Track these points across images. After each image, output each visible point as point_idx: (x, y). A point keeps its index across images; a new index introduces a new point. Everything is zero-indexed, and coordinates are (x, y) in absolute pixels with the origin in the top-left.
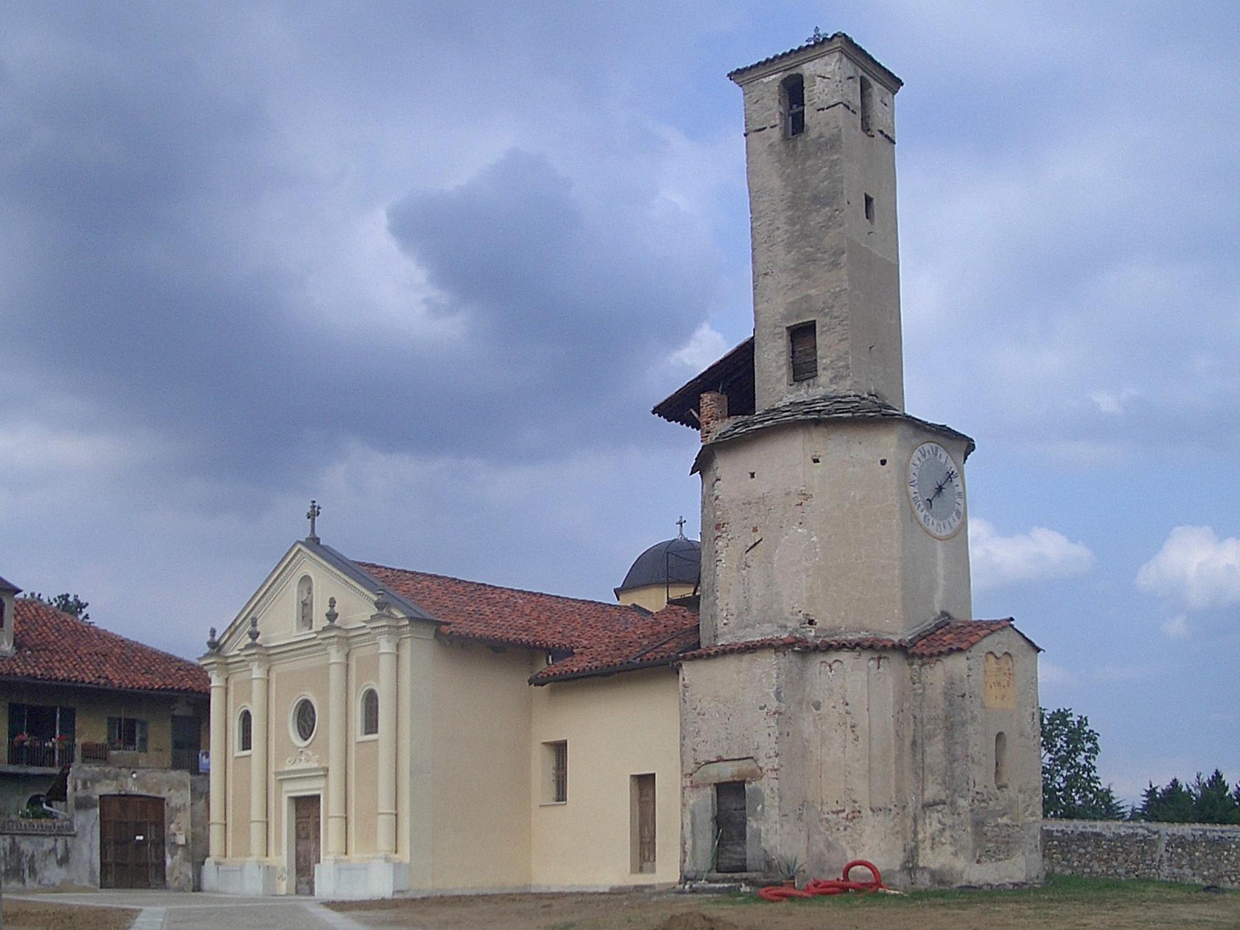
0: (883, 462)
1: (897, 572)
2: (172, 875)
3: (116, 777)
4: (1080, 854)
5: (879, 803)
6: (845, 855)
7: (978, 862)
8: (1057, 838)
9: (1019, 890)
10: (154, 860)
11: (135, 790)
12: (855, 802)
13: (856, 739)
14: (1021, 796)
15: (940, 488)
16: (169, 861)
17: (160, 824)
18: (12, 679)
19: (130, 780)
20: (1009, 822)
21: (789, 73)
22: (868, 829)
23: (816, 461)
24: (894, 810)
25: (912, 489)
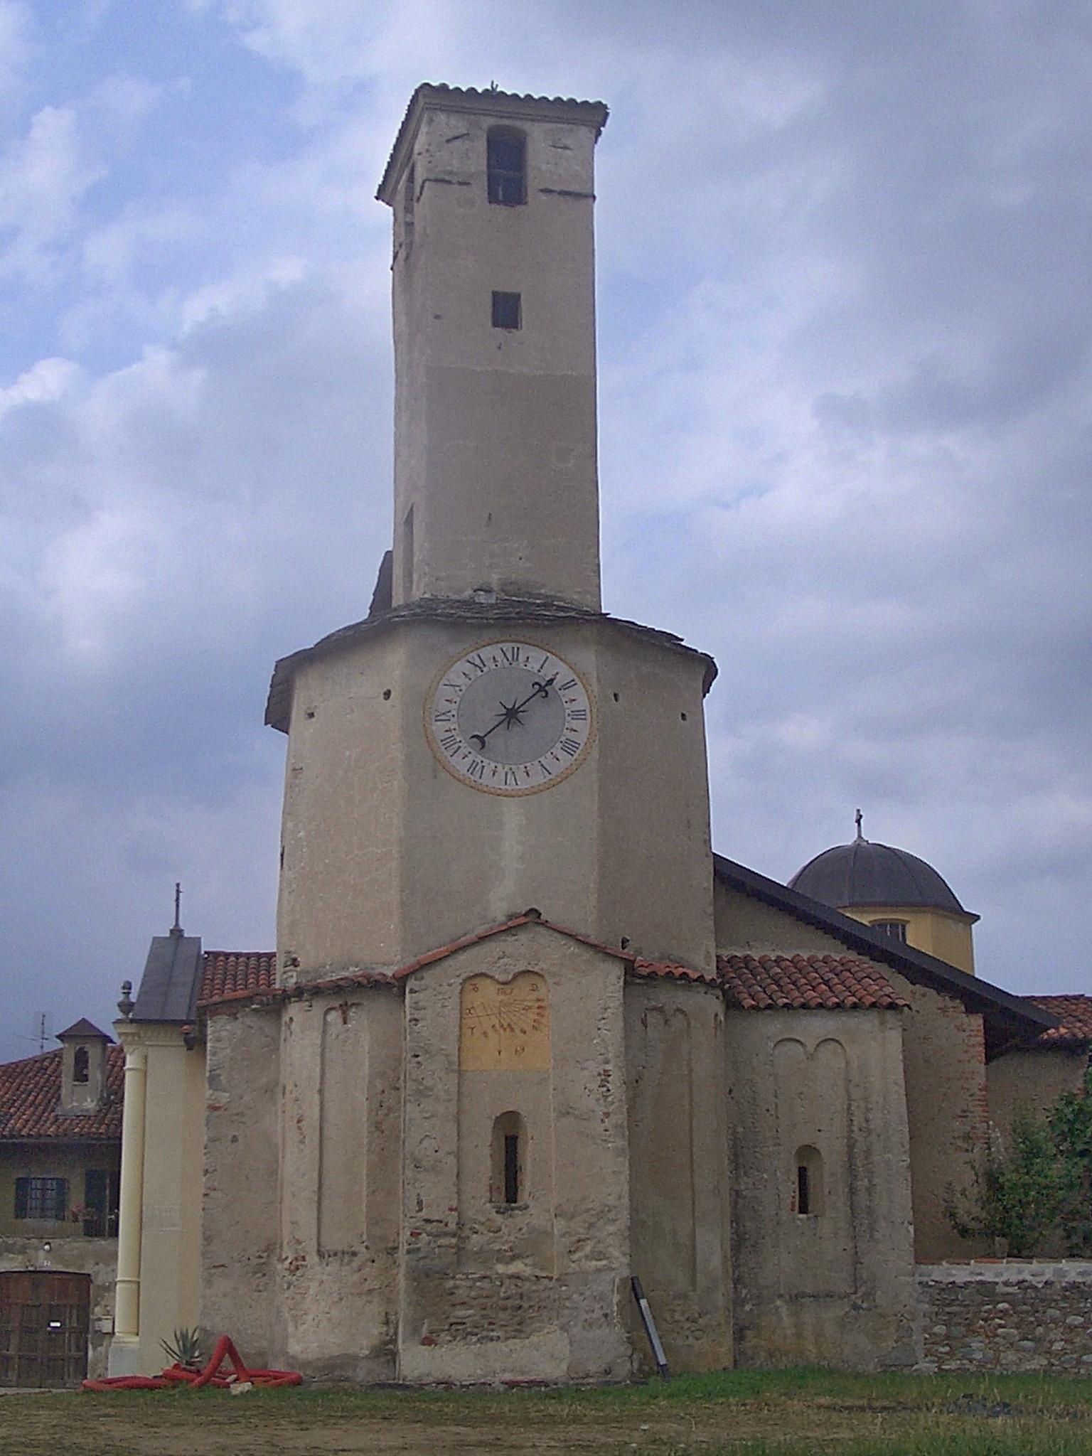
0: (387, 695)
1: (394, 864)
2: (94, 1370)
3: (23, 1250)
4: (1072, 1328)
5: (335, 1240)
6: (285, 1329)
7: (428, 1341)
8: (1006, 1297)
9: (572, 1389)
10: (73, 1353)
11: (47, 1264)
12: (299, 1242)
13: (302, 1142)
14: (560, 1225)
15: (512, 715)
16: (90, 1353)
17: (84, 1309)
18: (42, 1140)
19: (41, 1253)
20: (528, 1271)
21: (506, 122)
22: (314, 1287)
23: (311, 715)
24: (364, 1255)
25: (439, 729)
